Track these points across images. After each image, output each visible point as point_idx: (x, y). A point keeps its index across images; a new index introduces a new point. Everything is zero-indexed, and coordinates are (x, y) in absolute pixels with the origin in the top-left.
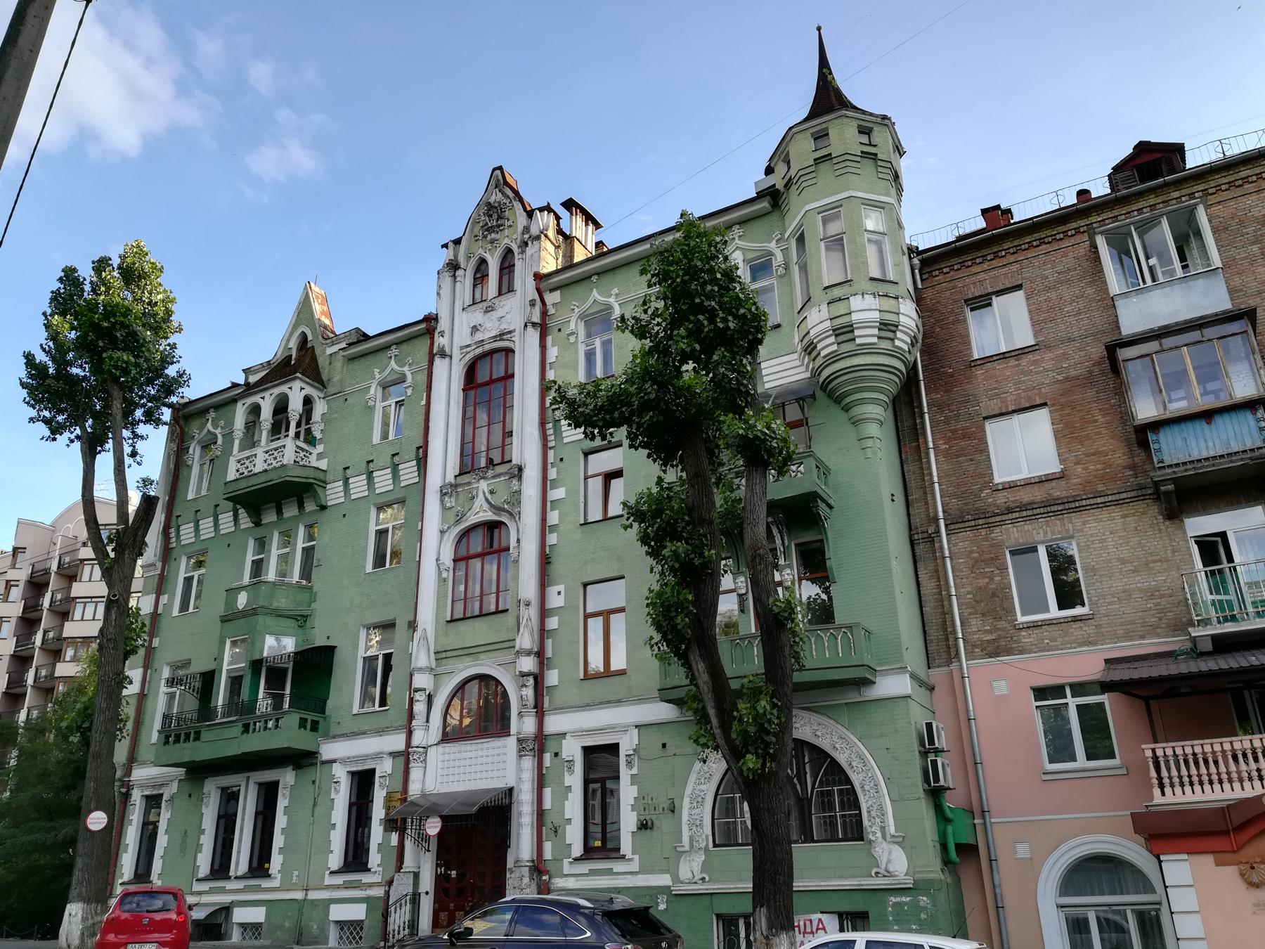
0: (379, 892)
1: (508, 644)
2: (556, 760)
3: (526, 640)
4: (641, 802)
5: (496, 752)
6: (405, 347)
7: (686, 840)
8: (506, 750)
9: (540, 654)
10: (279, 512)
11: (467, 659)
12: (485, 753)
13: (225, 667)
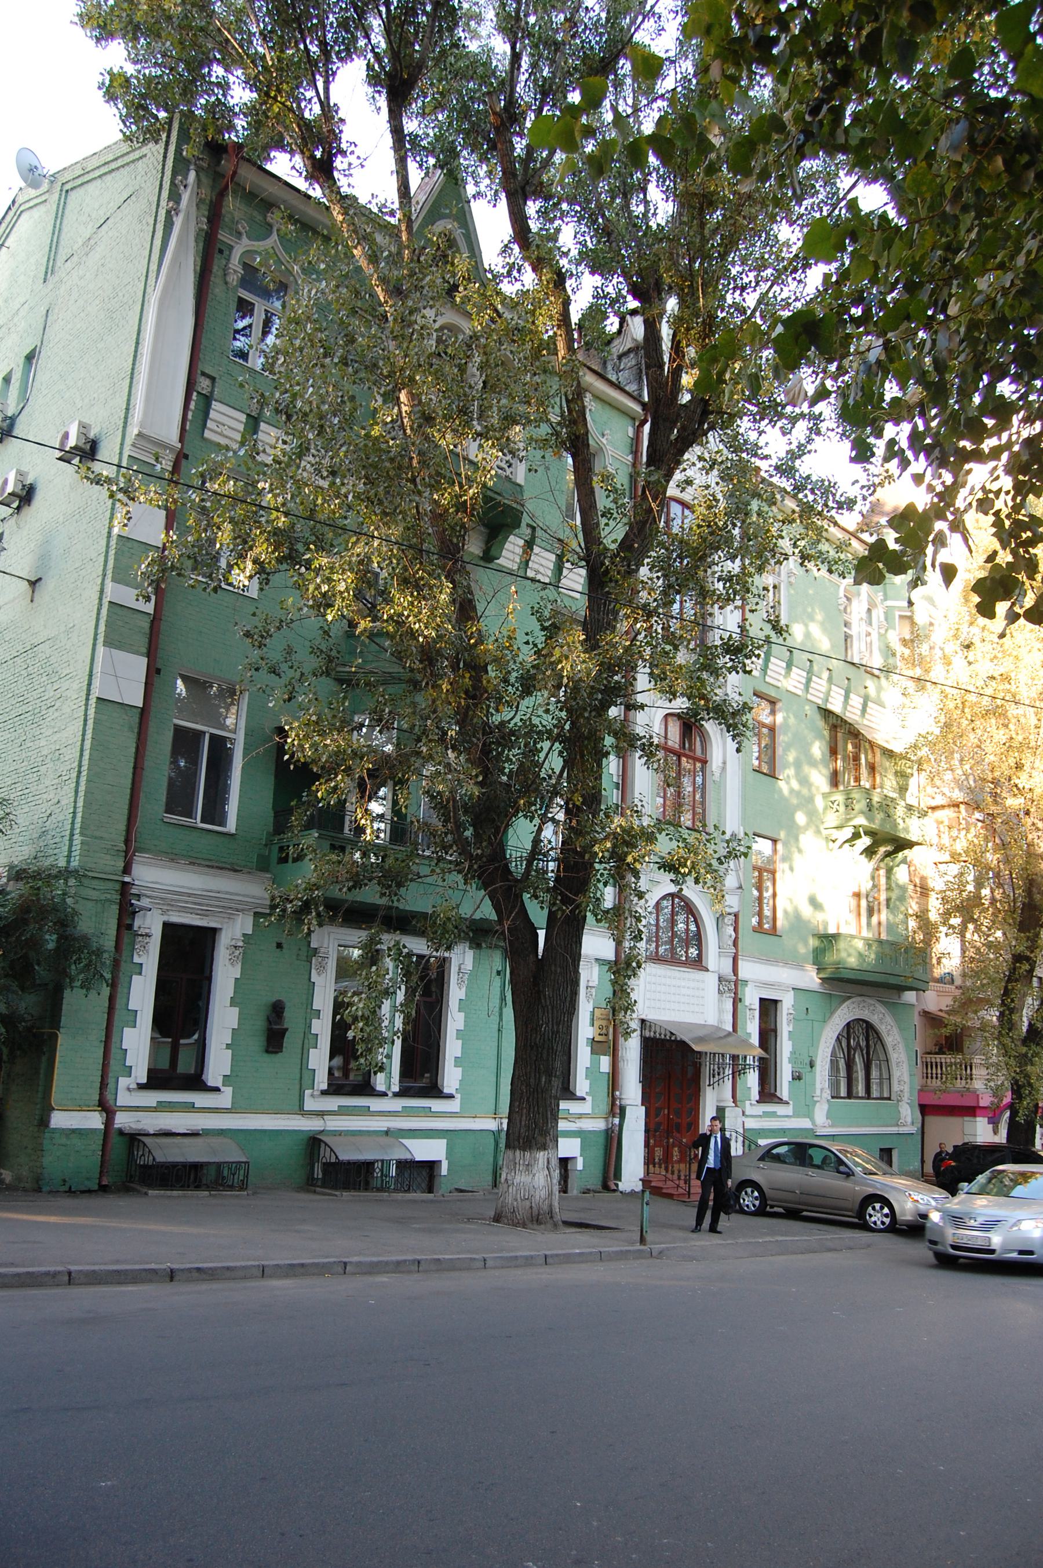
0: (600, 1125)
4: (794, 1059)
7: (818, 1092)
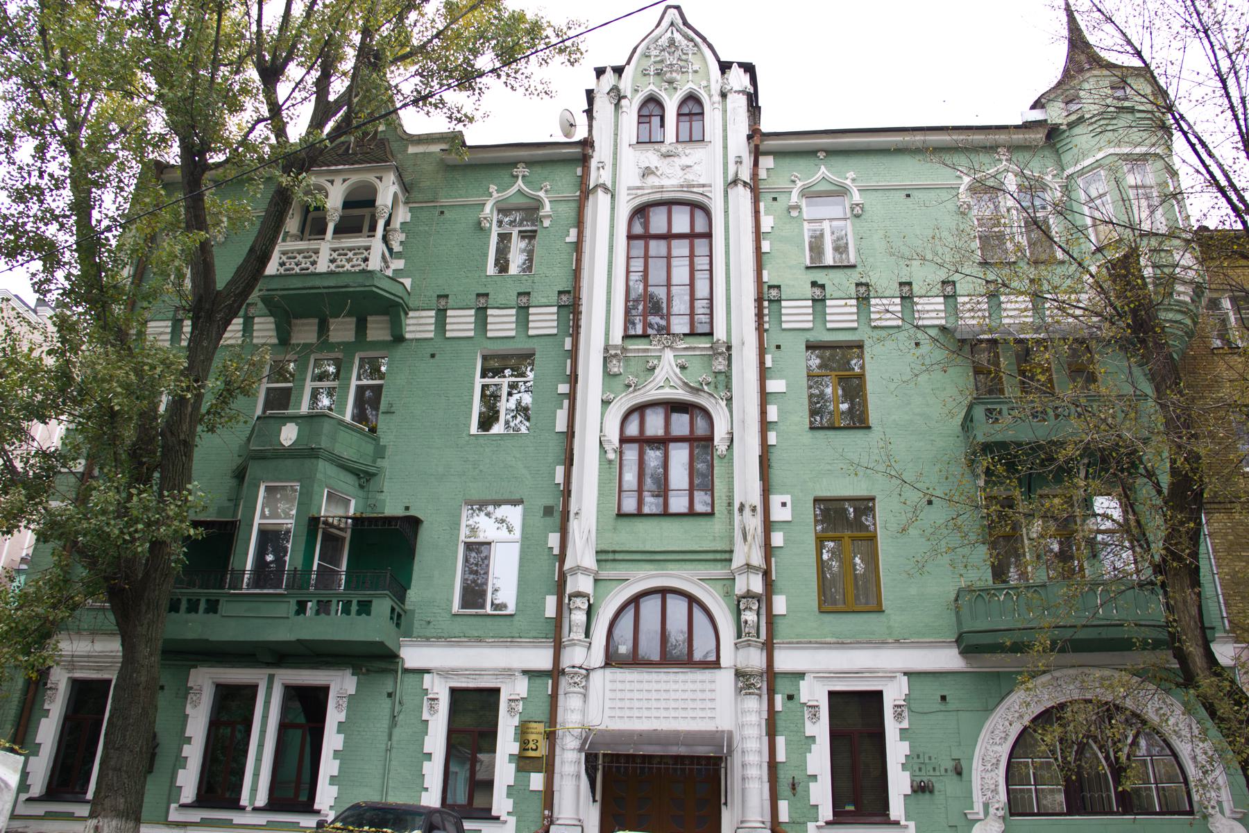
1: (726, 556)
2: (790, 704)
3: (748, 552)
5: (698, 686)
6: (538, 170)
7: (978, 807)
8: (713, 686)
9: (767, 574)
10: (323, 328)
11: (648, 566)
12: (680, 686)
13: (257, 520)
